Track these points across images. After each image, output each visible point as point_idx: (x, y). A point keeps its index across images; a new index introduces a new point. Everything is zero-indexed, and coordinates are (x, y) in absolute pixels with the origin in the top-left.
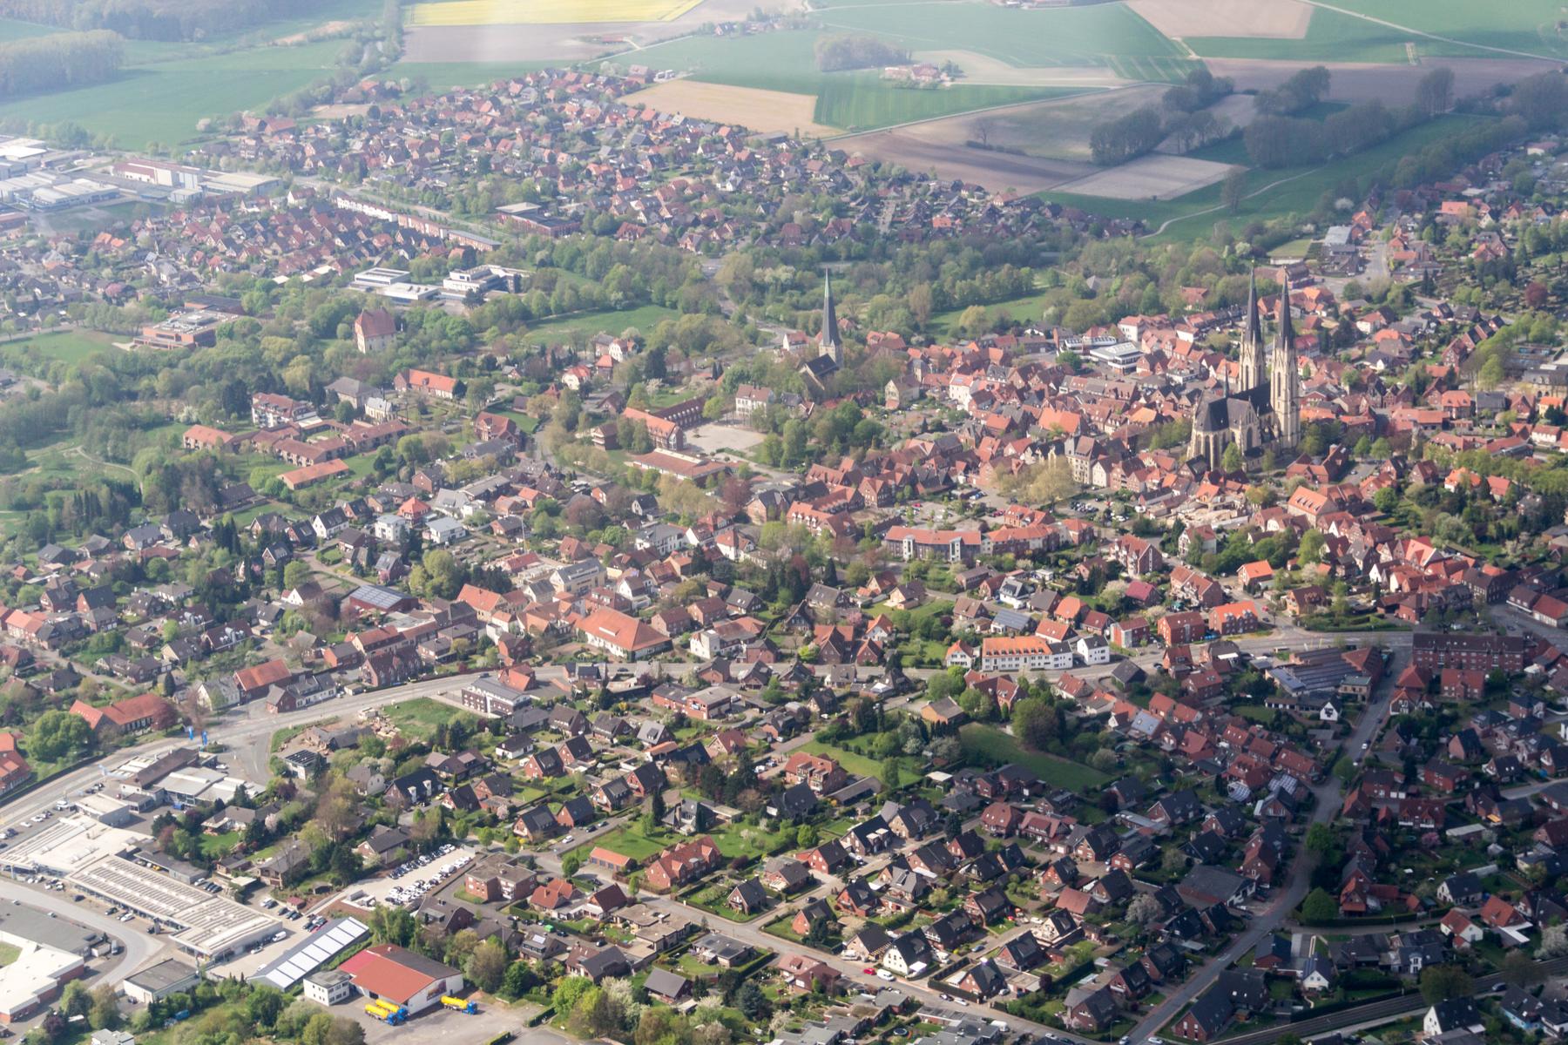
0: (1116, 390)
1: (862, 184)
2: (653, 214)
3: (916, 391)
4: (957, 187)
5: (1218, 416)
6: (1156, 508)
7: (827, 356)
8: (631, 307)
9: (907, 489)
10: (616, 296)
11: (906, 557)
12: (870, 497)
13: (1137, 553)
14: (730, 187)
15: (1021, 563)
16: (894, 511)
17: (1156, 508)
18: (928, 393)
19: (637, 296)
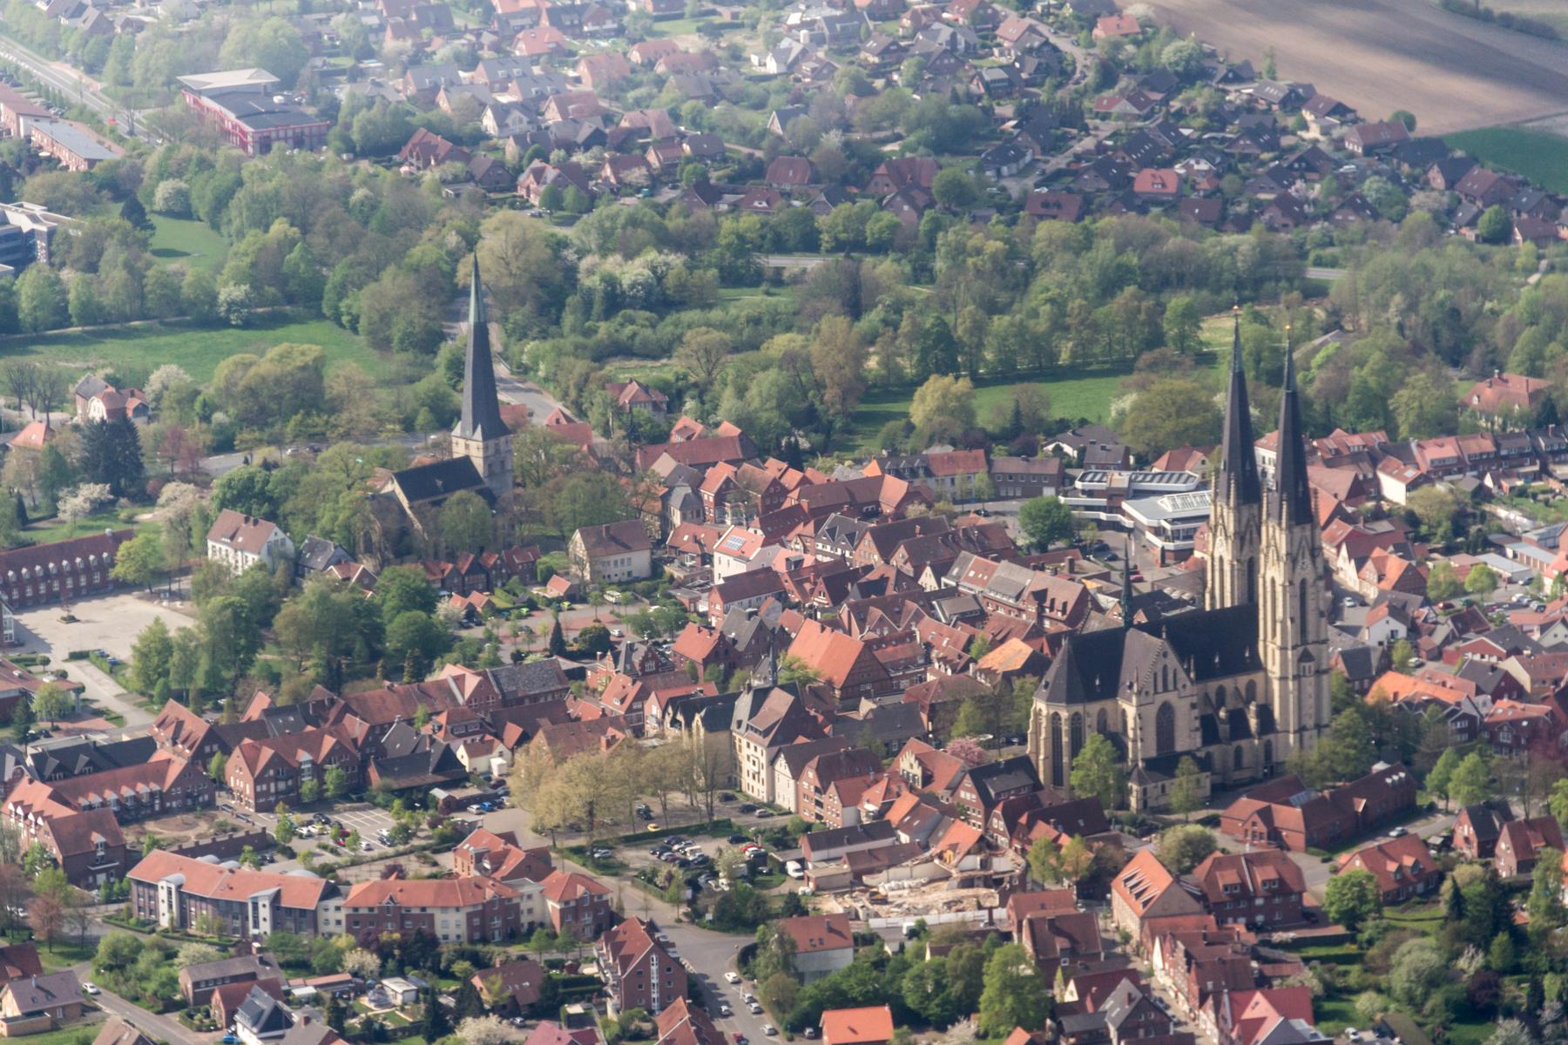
0: (1040, 596)
1: (1091, 77)
2: (516, 114)
3: (640, 561)
4: (1294, 100)
5: (1091, 665)
6: (833, 868)
7: (466, 460)
8: (275, 321)
9: (332, 774)
10: (230, 292)
11: (164, 922)
12: (240, 779)
13: (625, 961)
14: (772, 67)
15: (353, 959)
16: (270, 823)
17: (833, 868)
18: (670, 569)
19: (291, 299)
